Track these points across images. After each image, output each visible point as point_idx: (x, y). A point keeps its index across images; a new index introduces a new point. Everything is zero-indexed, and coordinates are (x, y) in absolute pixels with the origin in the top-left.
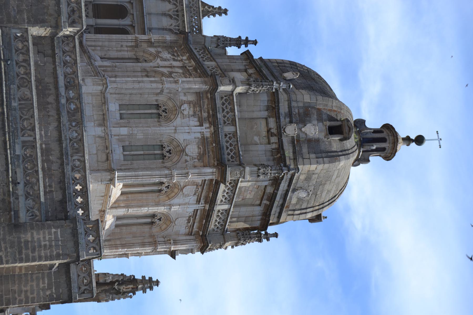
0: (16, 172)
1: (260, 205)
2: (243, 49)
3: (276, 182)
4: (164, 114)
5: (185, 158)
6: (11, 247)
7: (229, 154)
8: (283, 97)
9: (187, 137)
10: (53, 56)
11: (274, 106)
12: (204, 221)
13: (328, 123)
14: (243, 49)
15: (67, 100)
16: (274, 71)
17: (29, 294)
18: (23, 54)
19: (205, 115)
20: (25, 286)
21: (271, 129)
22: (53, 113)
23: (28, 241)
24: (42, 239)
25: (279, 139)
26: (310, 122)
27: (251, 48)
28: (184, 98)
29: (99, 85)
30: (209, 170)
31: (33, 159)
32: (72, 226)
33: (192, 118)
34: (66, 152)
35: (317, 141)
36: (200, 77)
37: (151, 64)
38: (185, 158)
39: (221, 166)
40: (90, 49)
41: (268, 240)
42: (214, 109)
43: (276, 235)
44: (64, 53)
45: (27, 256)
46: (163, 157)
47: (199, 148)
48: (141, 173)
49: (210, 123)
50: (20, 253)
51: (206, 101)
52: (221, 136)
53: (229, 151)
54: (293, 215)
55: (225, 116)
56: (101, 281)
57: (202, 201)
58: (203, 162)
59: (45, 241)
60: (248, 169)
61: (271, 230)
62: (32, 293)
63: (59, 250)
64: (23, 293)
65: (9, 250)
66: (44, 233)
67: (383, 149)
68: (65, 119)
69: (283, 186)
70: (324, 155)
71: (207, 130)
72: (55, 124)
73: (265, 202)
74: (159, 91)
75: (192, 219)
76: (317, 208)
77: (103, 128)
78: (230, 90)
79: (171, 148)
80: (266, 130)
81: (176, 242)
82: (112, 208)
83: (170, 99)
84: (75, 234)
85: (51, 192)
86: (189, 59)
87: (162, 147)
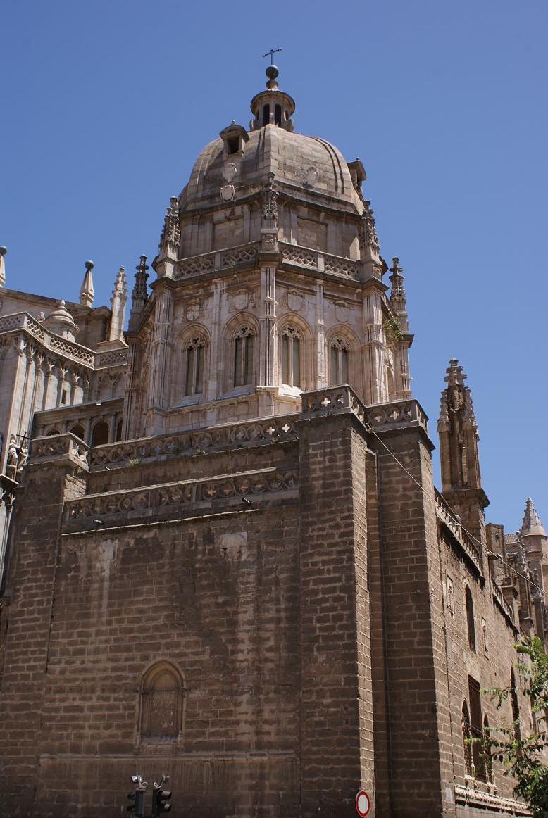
0: (234, 506)
1: (326, 225)
2: (150, 271)
4: (198, 341)
5: (250, 310)
6: (330, 507)
11: (199, 216)
12: (341, 286)
13: (225, 155)
15: (163, 453)
17: (408, 485)
19: (201, 291)
20: (397, 491)
21: (226, 217)
23: (323, 483)
24: (321, 466)
25: (237, 205)
26: (221, 175)
27: (149, 263)
28: (181, 318)
29: (154, 418)
31: (220, 485)
32: (306, 428)
34: (225, 446)
41: (371, 212)
42: (193, 281)
45: (343, 484)
46: (250, 337)
47: (240, 293)
49: (210, 284)
50: (338, 493)
51: (184, 292)
53: (244, 258)
54: (343, 188)
57: (314, 288)
58: (256, 287)
59: (324, 461)
63: (336, 442)
64: (408, 493)
65: (334, 508)
66: (314, 463)
69: (298, 196)
71: (219, 286)
72: (190, 464)
74: (169, 349)
75: (338, 302)
76: (336, 162)
77: (208, 411)
78: (173, 266)
79: (239, 328)
80: (227, 223)
81: (370, 320)
83: (180, 335)
87: (238, 340)
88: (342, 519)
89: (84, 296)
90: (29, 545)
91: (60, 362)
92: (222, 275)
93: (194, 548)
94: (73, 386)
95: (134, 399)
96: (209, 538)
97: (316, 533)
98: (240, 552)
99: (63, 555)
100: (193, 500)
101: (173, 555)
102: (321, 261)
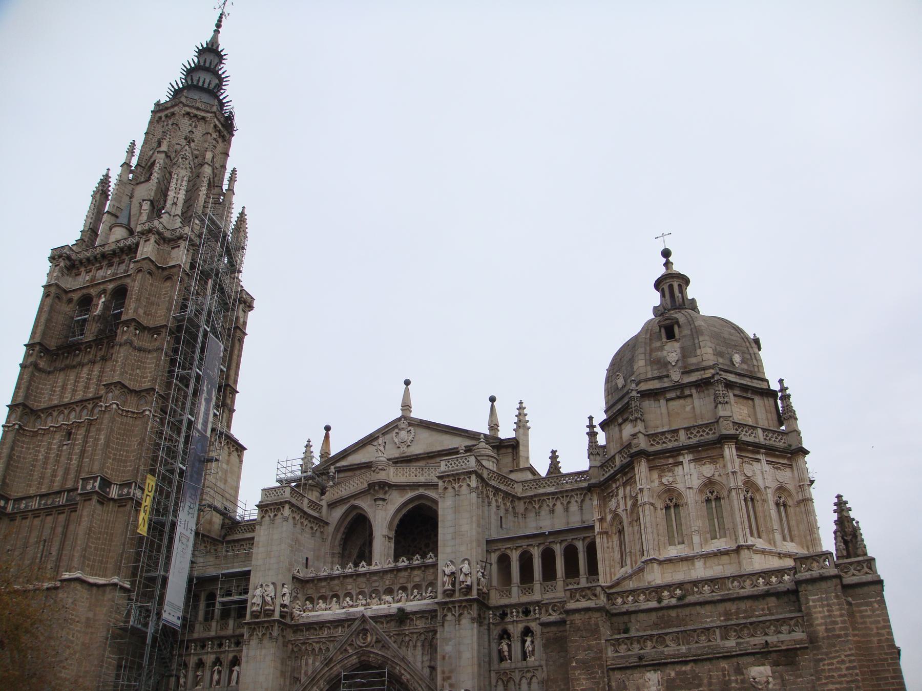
1: (753, 400)
2: (598, 429)
3: (729, 385)
4: (674, 501)
6: (834, 646)
7: (708, 434)
8: (644, 387)
9: (695, 477)
10: (628, 613)
13: (664, 340)
14: (598, 429)
15: (672, 597)
16: (617, 397)
17: (880, 625)
18: (631, 644)
19: (671, 461)
20: (871, 629)
22: (687, 611)
27: (596, 422)
28: (656, 482)
30: (727, 452)
33: (676, 473)
35: (682, 348)
36: (633, 468)
37: (624, 517)
38: (716, 477)
39: (723, 440)
40: (615, 578)
41: (787, 388)
43: (781, 381)
44: (624, 603)
46: (718, 499)
47: (705, 464)
48: (738, 520)
50: (839, 636)
51: (657, 461)
52: (689, 442)
55: (670, 440)
56: (845, 553)
57: (758, 457)
60: (721, 413)
61: (775, 386)
62: (879, 622)
66: (815, 613)
67: (680, 286)
68: (691, 599)
69: (732, 378)
70: (696, 341)
71: (686, 458)
72: (698, 608)
73: (749, 395)
82: (775, 546)
84: (813, 581)
85: (769, 609)
86: (615, 481)
87: (708, 501)
88: (846, 656)
89: (494, 427)
90: (579, 674)
91: (497, 490)
92: (690, 448)
93: (727, 678)
94: (507, 510)
95: (605, 540)
96: (739, 671)
97: (826, 667)
98: (768, 682)
99: (613, 684)
100: (719, 640)
101: (710, 684)
102: (760, 431)
